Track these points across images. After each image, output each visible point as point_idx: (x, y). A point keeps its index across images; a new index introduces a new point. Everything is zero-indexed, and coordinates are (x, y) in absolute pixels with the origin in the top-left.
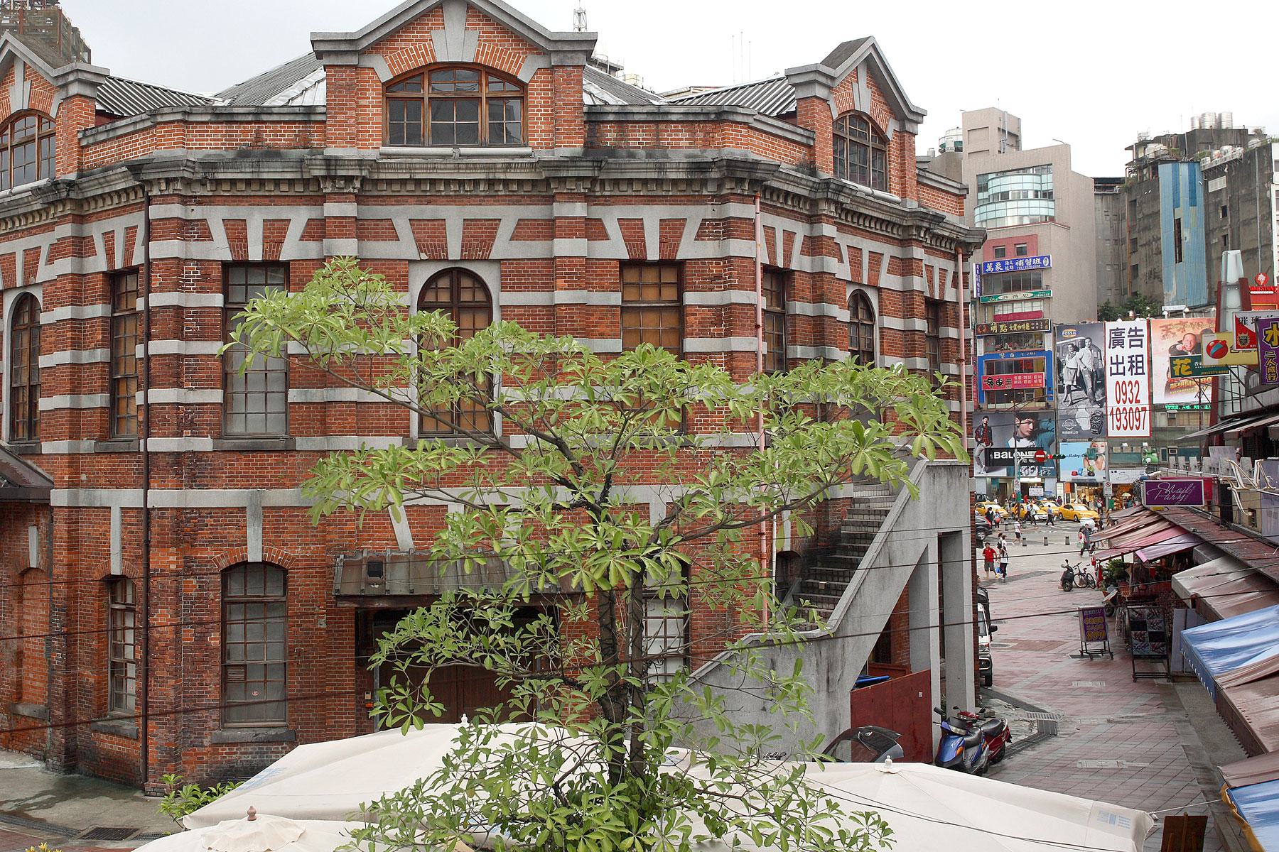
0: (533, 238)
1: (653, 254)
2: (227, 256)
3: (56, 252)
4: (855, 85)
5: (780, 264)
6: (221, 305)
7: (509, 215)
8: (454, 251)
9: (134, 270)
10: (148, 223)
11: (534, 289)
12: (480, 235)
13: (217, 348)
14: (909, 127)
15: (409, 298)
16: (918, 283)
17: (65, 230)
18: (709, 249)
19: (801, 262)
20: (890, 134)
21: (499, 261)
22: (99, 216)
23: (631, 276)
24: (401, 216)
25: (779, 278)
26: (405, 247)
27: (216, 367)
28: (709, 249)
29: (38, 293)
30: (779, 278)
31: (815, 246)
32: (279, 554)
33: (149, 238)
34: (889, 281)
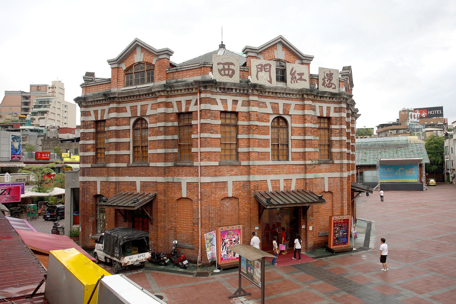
0: (299, 109)
1: (325, 115)
2: (223, 109)
7: (293, 103)
13: (219, 136)
15: (269, 124)
17: (163, 100)
18: (337, 115)
22: (175, 96)
24: (268, 101)
26: (269, 110)
27: (219, 141)
28: (337, 115)
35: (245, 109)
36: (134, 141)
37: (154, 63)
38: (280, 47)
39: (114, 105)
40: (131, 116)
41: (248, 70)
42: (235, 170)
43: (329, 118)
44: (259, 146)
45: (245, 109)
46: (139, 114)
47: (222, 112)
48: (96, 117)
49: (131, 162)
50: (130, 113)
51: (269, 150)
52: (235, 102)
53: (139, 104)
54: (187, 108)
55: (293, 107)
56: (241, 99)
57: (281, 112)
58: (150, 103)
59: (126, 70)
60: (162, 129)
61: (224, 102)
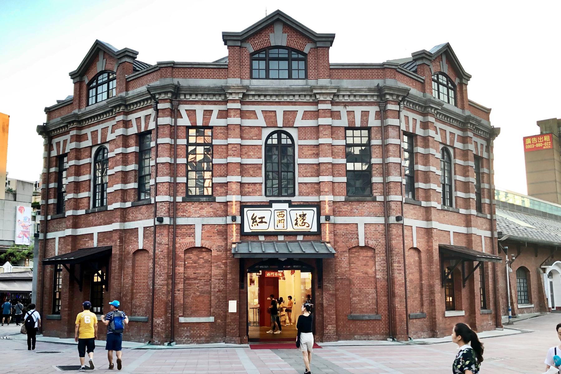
1: (358, 124)
3: (114, 128)
4: (441, 62)
5: (411, 131)
6: (186, 143)
7: (301, 110)
8: (280, 123)
9: (150, 132)
10: (157, 110)
11: (311, 139)
12: (289, 116)
14: (464, 81)
15: (262, 142)
16: (471, 147)
17: (120, 118)
19: (419, 132)
20: (456, 83)
23: (349, 133)
24: (258, 109)
25: (412, 136)
29: (107, 146)
30: (412, 136)
31: (425, 125)
32: (207, 244)
33: (157, 116)
34: (458, 145)
35: (222, 122)
36: (95, 177)
37: (115, 71)
38: (278, 28)
39: (73, 133)
41: (226, 67)
42: (207, 209)
43: (369, 129)
44: (242, 174)
45: (222, 122)
46: (99, 142)
47: (188, 128)
48: (58, 151)
49: (91, 208)
50: (91, 141)
51: (261, 179)
52: (208, 113)
53: (99, 128)
54: (146, 126)
55: (300, 115)
56: (216, 109)
58: (110, 124)
60: (118, 157)
61: (192, 114)
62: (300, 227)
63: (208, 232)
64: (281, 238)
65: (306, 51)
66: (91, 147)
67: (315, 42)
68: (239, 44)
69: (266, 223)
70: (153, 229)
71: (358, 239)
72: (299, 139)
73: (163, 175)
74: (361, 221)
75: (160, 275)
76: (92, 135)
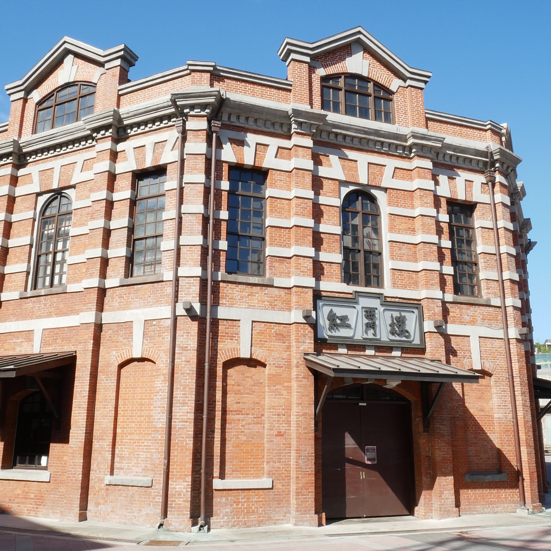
2: (233, 159)
10: (184, 133)
15: (338, 202)
21: (385, 190)
32: (258, 355)
40: (38, 190)
57: (363, 180)
59: (39, 103)
62: (398, 338)
63: (261, 333)
64: (370, 352)
65: (393, 88)
66: (38, 194)
67: (404, 79)
68: (308, 59)
69: (349, 326)
70: (169, 323)
71: (471, 358)
72: (390, 204)
73: (192, 234)
74: (474, 332)
75: (184, 404)
76: (40, 176)
